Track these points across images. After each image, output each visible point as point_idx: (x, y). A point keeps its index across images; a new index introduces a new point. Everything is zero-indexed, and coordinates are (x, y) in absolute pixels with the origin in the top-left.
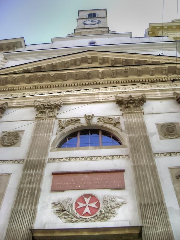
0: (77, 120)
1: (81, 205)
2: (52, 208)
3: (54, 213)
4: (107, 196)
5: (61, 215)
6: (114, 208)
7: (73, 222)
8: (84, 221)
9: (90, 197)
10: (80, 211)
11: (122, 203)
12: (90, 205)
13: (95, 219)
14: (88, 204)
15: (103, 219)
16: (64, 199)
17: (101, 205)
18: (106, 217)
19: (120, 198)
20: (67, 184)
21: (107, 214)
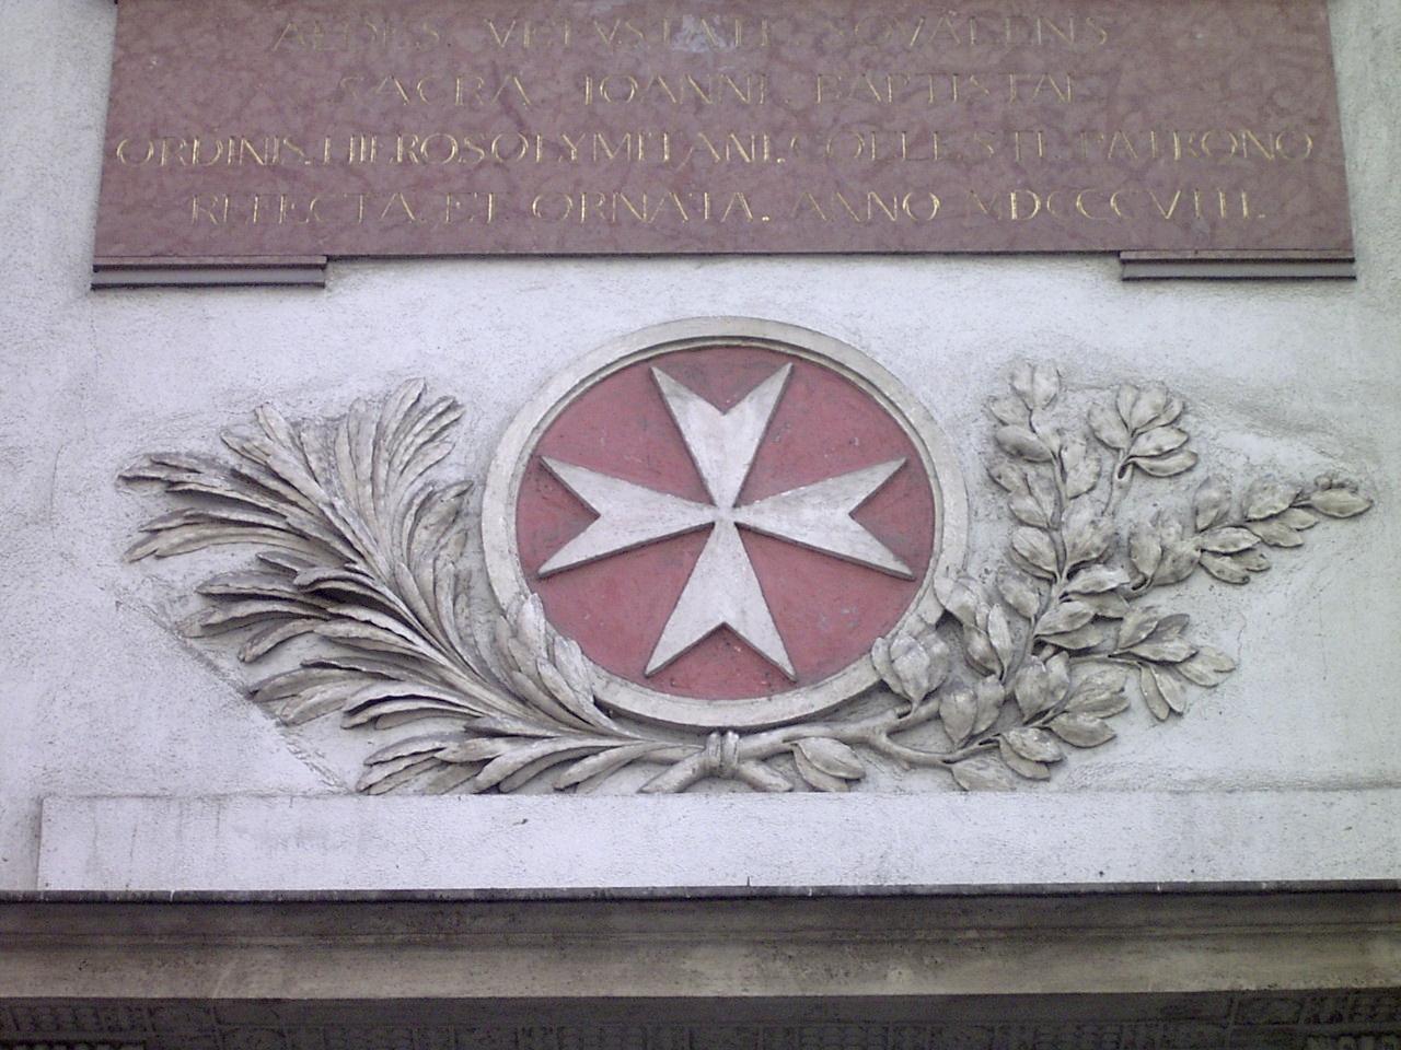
1: (625, 513)
2: (132, 557)
3: (178, 629)
4: (1045, 386)
5: (288, 661)
6: (1178, 580)
7: (495, 788)
8: (679, 774)
9: (772, 389)
10: (613, 600)
11: (1300, 502)
12: (766, 517)
13: (857, 743)
14: (743, 498)
15: (985, 743)
16: (336, 399)
17: (968, 533)
18: (1040, 718)
19: (1267, 416)
20: (362, 150)
21: (1058, 666)
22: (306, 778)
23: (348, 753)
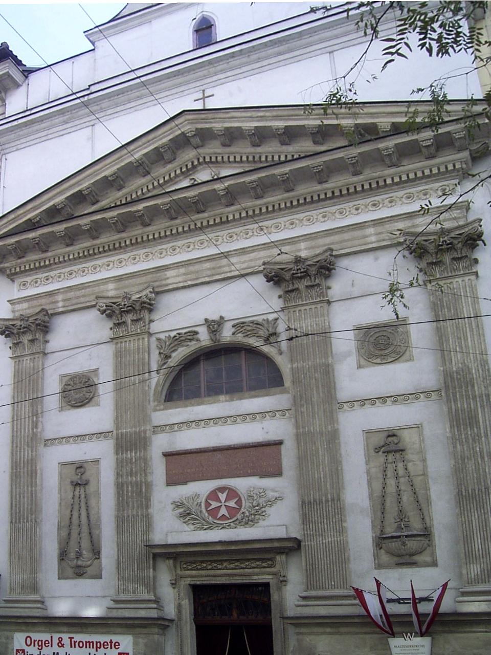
0: (193, 335)
20: (189, 471)
22: (189, 530)
23: (192, 527)
